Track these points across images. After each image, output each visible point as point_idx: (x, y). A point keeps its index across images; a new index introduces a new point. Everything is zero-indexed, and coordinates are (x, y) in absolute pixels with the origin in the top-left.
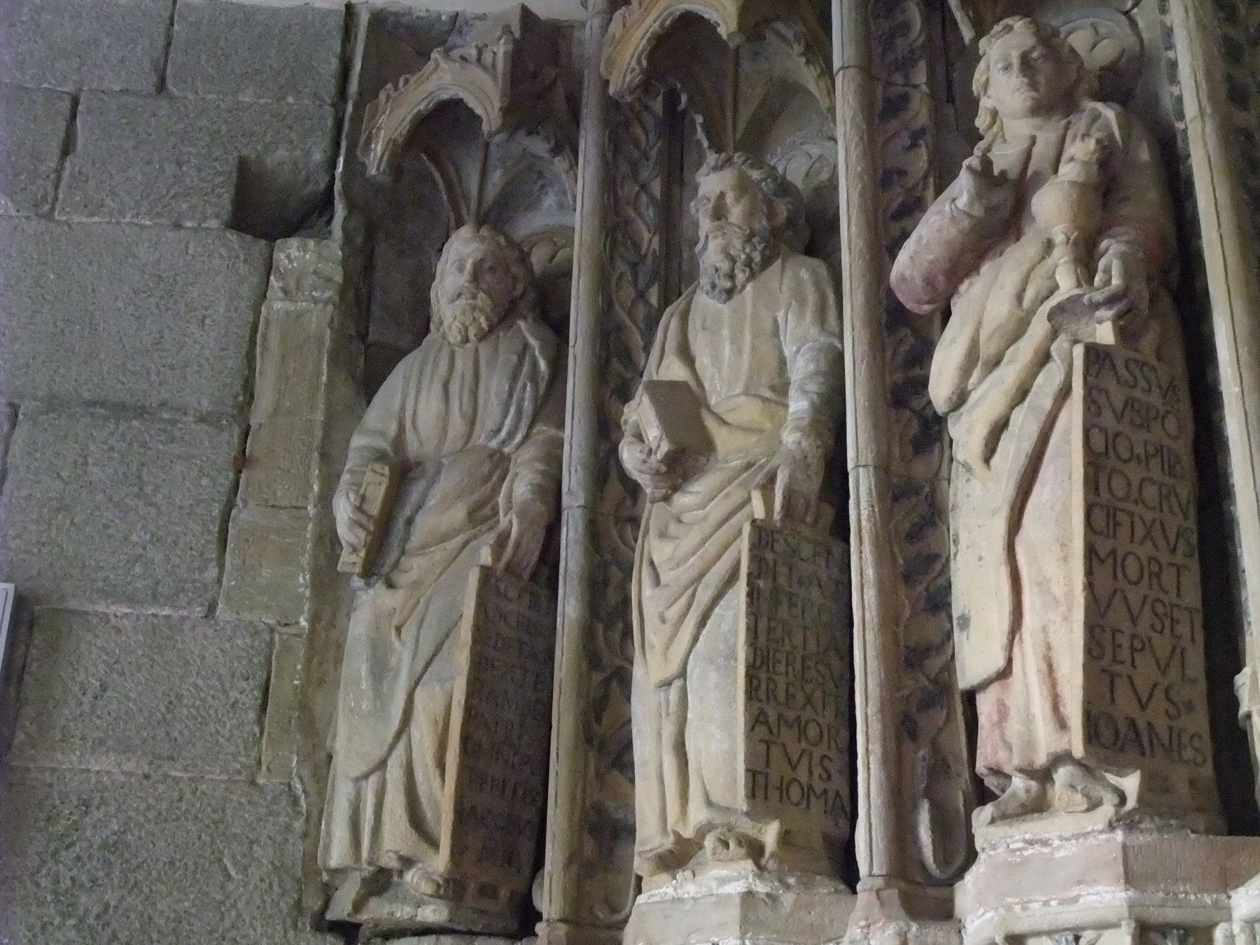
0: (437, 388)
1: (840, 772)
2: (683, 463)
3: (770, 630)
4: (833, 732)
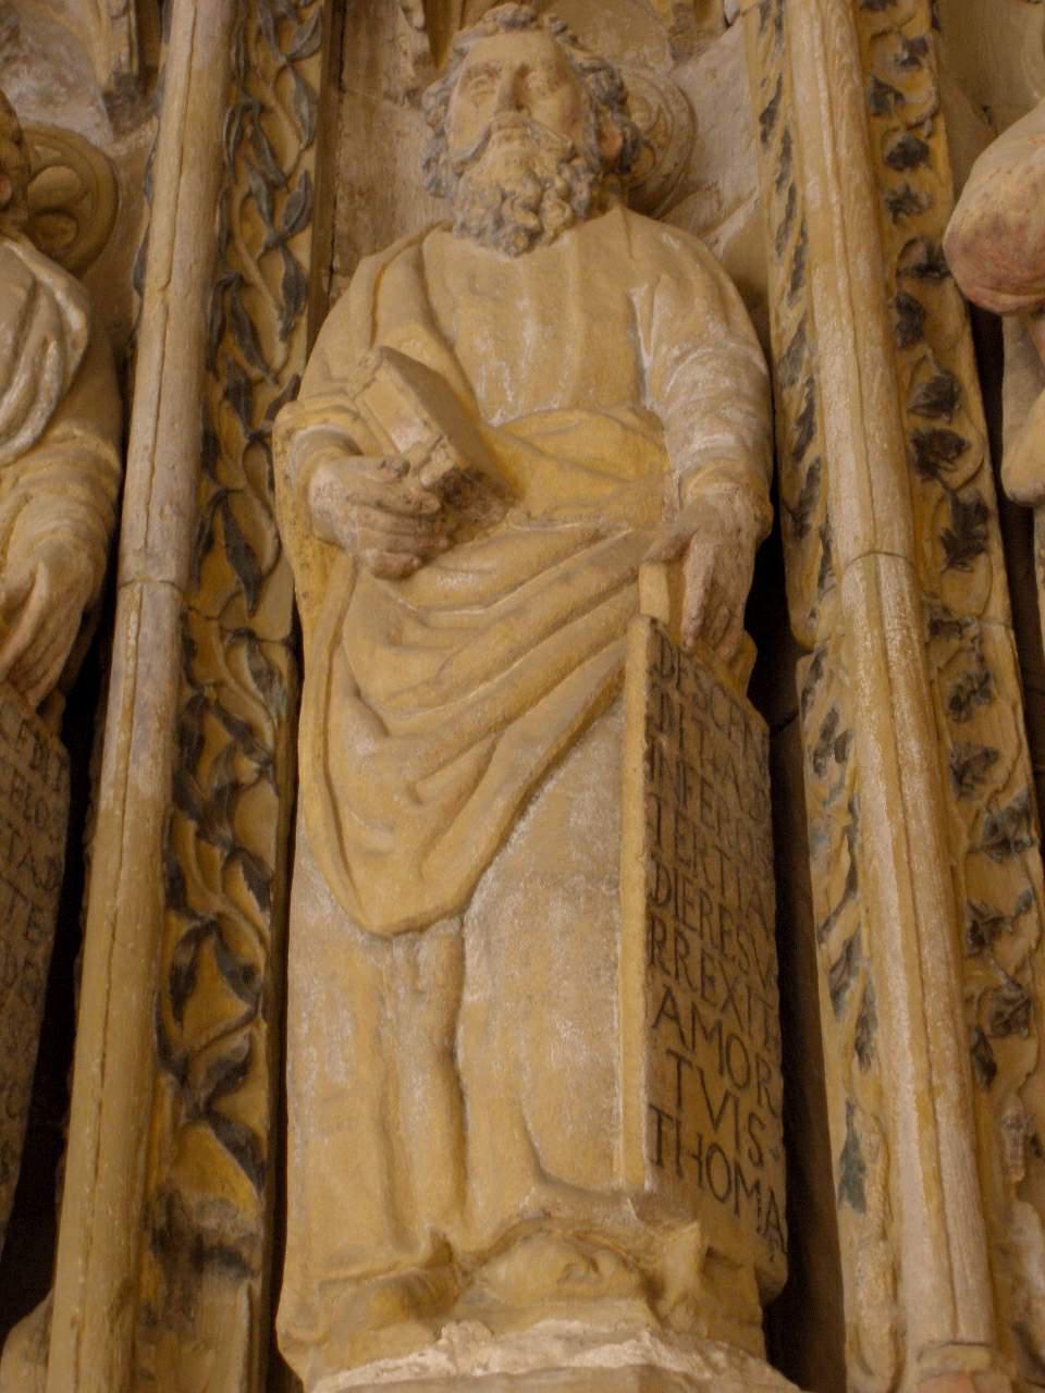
1: (776, 1158)
2: (463, 502)
3: (678, 839)
4: (763, 1071)
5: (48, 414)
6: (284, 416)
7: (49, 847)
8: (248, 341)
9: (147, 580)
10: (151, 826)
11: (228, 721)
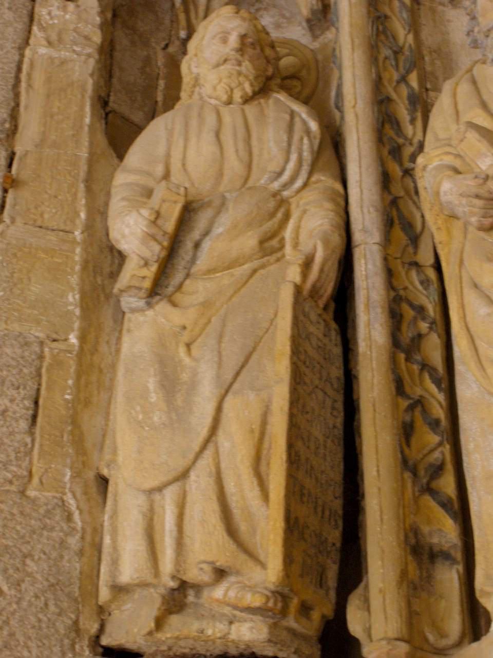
0: (208, 137)
5: (308, 171)
6: (420, 160)
7: (337, 372)
8: (395, 127)
9: (366, 243)
10: (385, 358)
11: (411, 305)
